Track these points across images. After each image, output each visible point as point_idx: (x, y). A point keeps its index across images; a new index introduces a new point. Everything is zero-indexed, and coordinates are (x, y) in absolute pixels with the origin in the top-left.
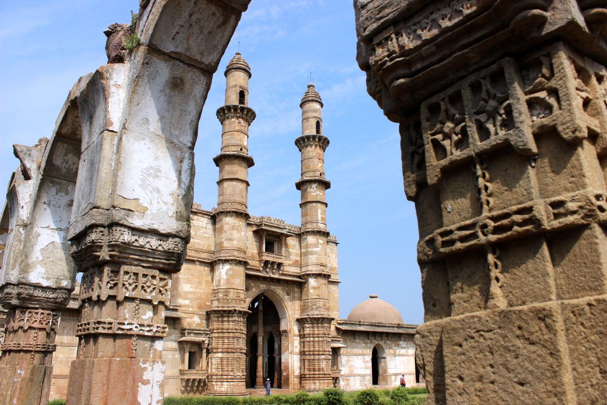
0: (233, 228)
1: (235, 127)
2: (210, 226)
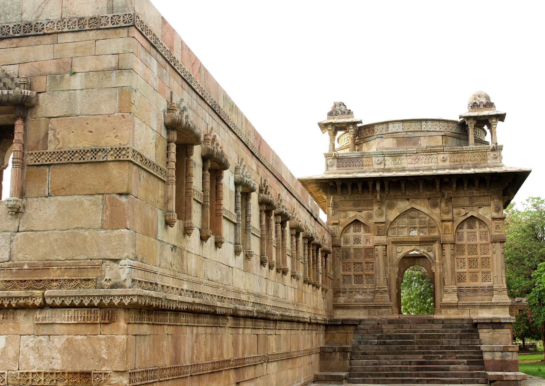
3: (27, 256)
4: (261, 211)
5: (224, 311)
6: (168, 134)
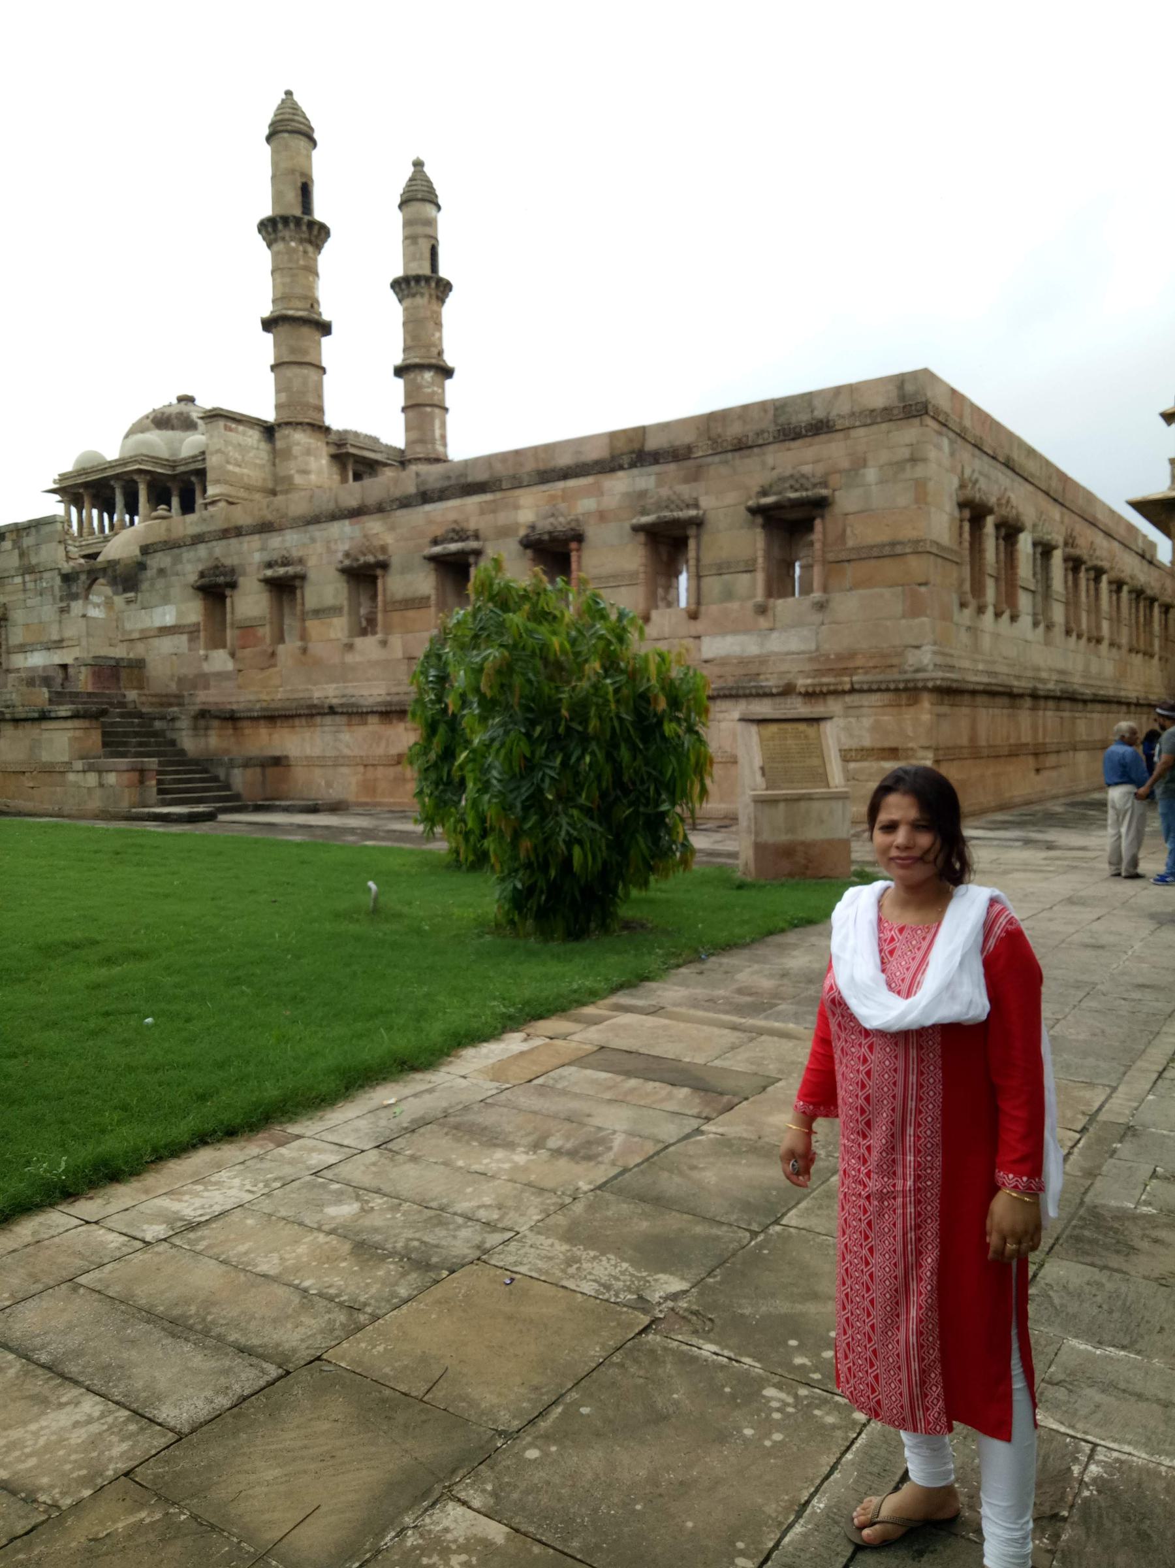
0: (308, 452)
1: (298, 260)
2: (264, 446)
3: (833, 646)
4: (1066, 570)
5: (1021, 691)
6: (961, 511)
